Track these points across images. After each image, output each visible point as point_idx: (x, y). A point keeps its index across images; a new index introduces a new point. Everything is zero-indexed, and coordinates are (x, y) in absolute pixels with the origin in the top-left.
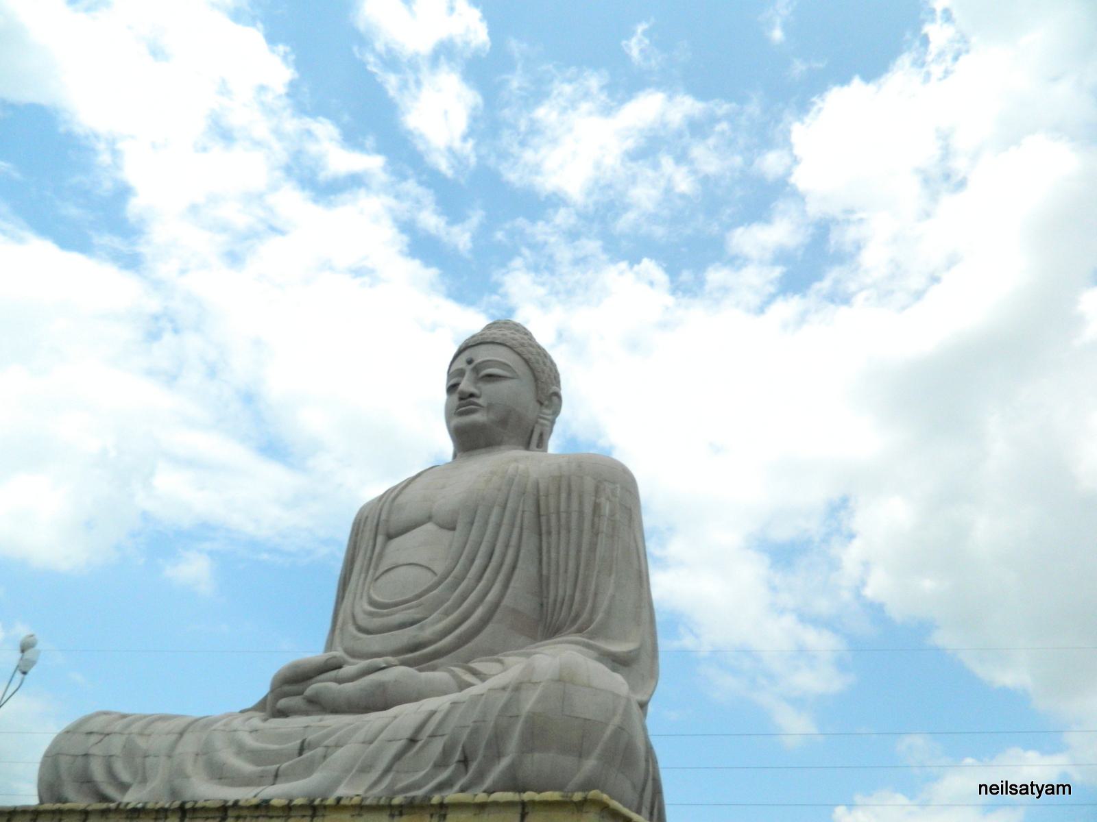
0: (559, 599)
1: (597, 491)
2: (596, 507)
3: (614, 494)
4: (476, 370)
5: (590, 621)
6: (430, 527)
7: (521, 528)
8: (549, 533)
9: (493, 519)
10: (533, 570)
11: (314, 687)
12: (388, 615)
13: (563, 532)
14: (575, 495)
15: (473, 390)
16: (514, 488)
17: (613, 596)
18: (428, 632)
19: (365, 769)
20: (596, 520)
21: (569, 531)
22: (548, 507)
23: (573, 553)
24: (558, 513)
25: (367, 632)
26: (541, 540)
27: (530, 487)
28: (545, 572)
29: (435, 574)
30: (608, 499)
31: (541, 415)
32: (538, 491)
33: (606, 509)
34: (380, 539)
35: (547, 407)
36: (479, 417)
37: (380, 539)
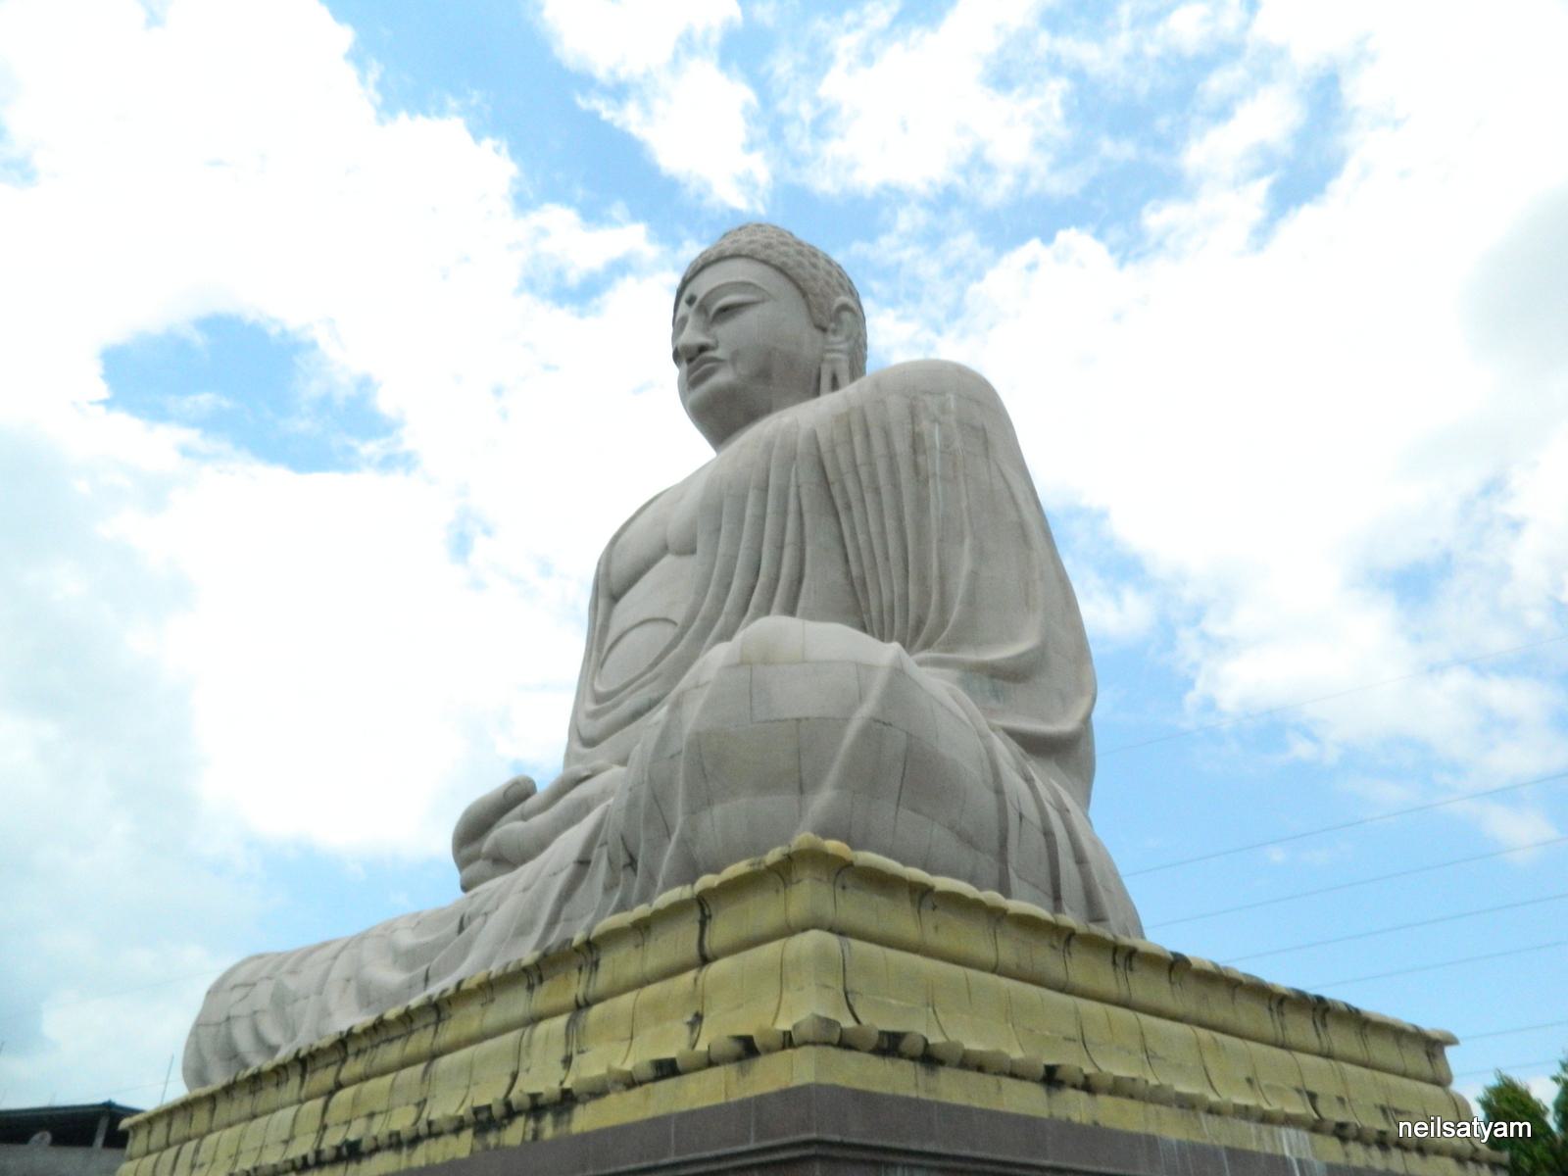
1: (913, 416)
2: (916, 443)
3: (943, 409)
4: (703, 309)
5: (942, 624)
6: (668, 560)
7: (800, 514)
8: (848, 507)
10: (837, 575)
12: (615, 706)
13: (869, 497)
16: (775, 452)
17: (974, 575)
20: (921, 459)
21: (877, 491)
22: (838, 468)
23: (890, 524)
26: (839, 524)
27: (801, 447)
28: (855, 571)
29: (675, 623)
30: (935, 420)
31: (827, 347)
32: (818, 449)
33: (935, 436)
35: (835, 332)
36: (722, 378)
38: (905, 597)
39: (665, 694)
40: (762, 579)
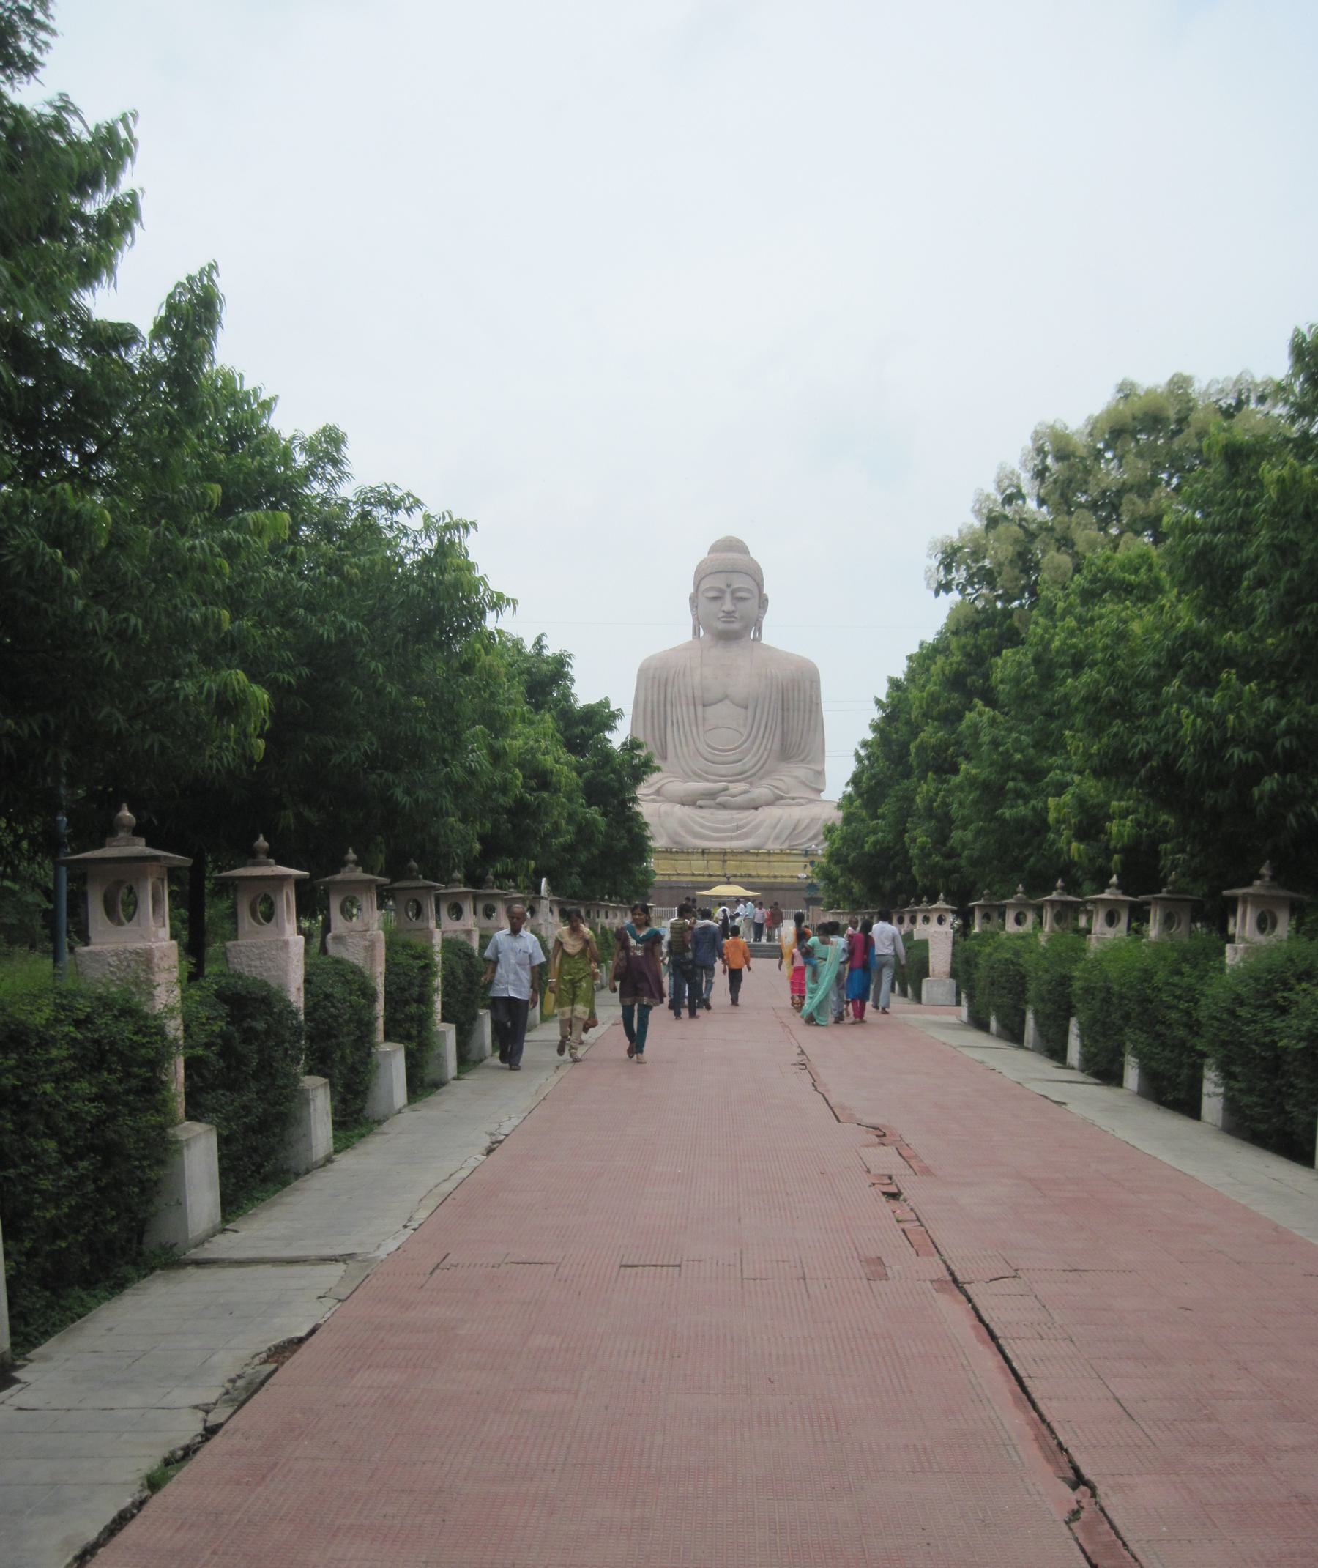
4: (733, 592)
6: (727, 702)
11: (720, 799)
18: (747, 766)
19: (777, 838)
34: (700, 708)
37: (700, 708)
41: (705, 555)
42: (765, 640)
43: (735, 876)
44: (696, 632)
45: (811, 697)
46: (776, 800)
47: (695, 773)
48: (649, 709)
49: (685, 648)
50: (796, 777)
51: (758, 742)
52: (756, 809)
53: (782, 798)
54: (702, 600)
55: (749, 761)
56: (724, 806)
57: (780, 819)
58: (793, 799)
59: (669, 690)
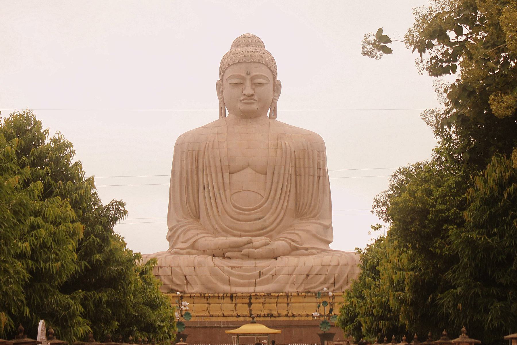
0: (305, 204)
4: (252, 79)
6: (249, 170)
8: (300, 175)
9: (282, 172)
13: (307, 177)
14: (311, 160)
15: (251, 92)
18: (267, 223)
23: (311, 185)
24: (304, 168)
25: (238, 220)
34: (226, 175)
36: (255, 107)
37: (226, 175)
38: (311, 203)
39: (264, 217)
40: (284, 192)
41: (229, 49)
42: (279, 118)
43: (259, 316)
44: (222, 113)
45: (319, 163)
46: (293, 250)
47: (224, 231)
48: (185, 176)
49: (214, 125)
50: (308, 231)
51: (276, 202)
52: (276, 258)
53: (297, 249)
54: (226, 86)
55: (269, 218)
56: (248, 257)
57: (296, 266)
58: (307, 249)
59: (200, 161)
